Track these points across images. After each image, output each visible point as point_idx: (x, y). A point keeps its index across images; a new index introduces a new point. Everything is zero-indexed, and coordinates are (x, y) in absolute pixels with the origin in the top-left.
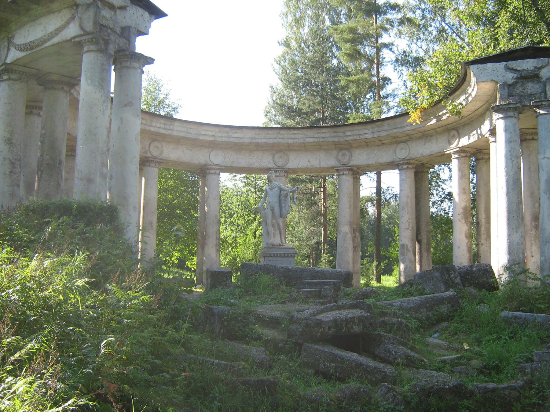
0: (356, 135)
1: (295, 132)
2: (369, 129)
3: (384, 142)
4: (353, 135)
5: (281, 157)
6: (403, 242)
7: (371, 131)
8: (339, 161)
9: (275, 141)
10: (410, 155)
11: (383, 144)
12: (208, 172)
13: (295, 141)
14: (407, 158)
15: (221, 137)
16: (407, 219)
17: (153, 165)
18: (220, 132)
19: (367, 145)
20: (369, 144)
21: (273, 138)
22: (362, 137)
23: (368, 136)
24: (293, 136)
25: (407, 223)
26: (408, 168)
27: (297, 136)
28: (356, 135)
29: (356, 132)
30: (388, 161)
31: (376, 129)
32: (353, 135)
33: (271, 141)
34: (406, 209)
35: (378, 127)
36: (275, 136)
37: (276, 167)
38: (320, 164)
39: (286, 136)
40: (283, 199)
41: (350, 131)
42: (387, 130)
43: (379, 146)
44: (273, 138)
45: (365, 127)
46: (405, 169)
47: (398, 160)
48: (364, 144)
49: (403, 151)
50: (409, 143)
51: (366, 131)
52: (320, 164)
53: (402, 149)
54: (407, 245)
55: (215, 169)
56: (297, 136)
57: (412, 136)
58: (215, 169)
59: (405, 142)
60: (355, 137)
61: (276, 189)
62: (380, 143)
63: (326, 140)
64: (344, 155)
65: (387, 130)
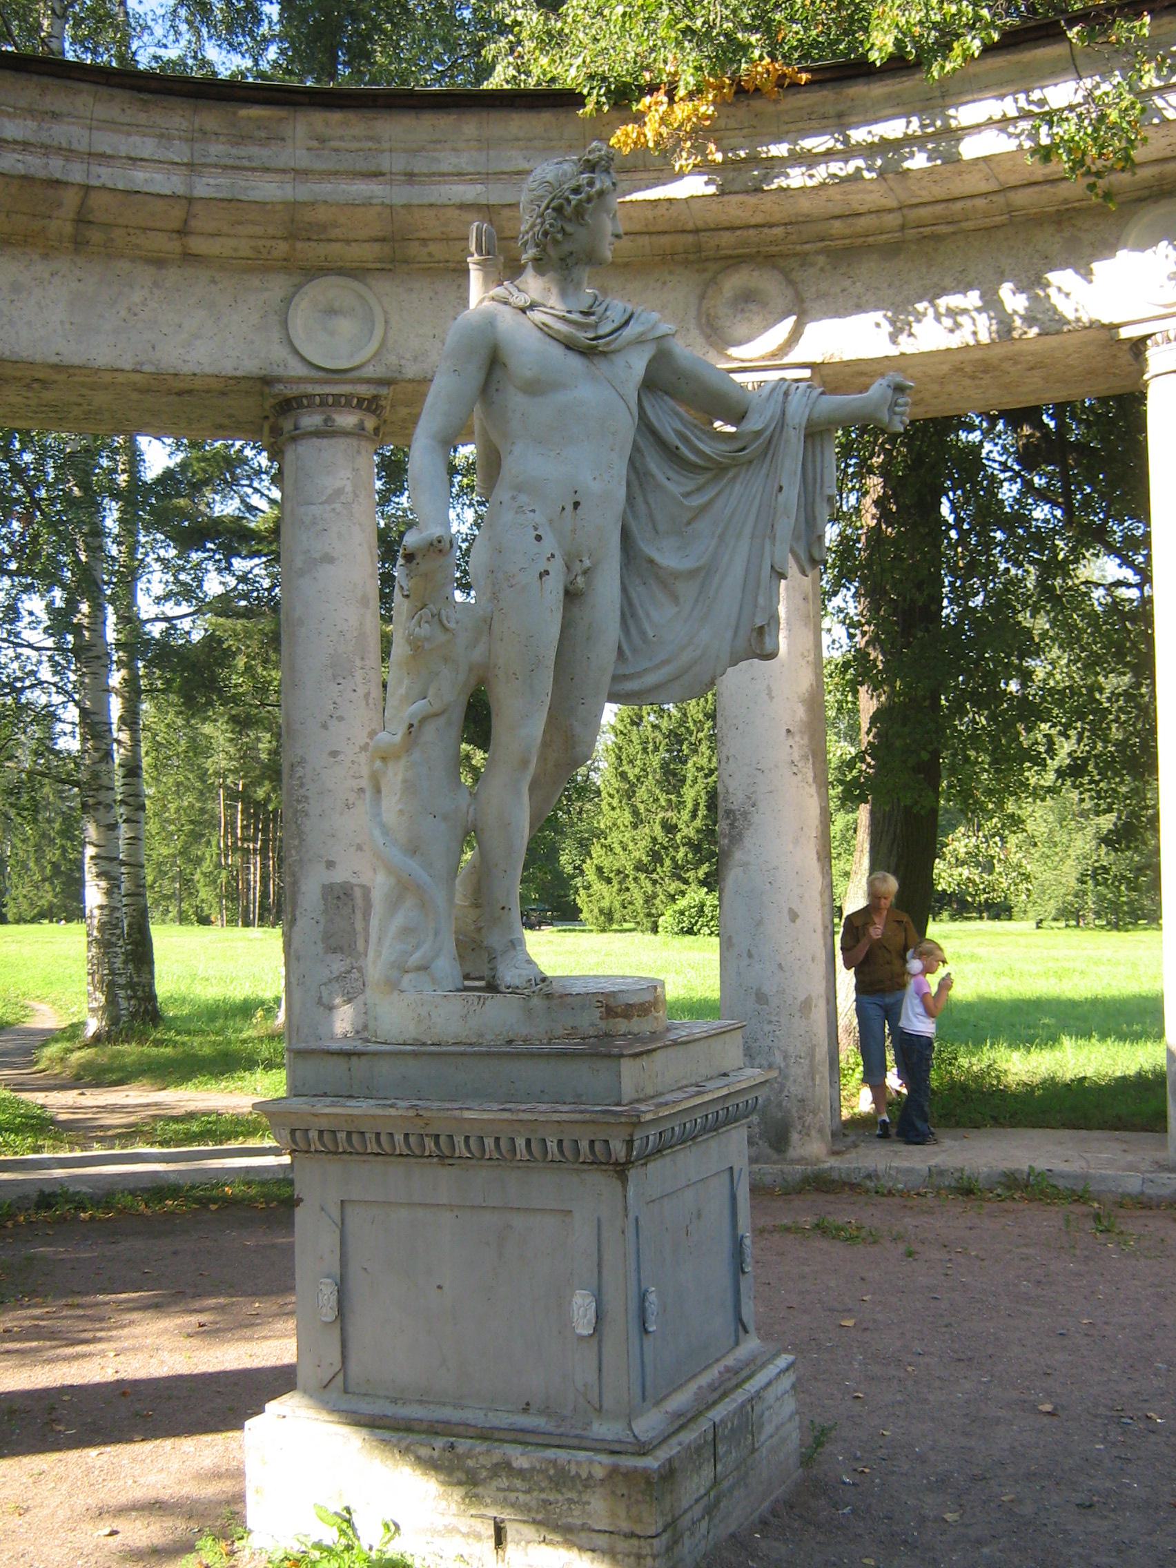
0: (69, 153)
2: (164, 137)
3: (197, 245)
4: (47, 149)
6: (340, 875)
7: (179, 152)
10: (392, 359)
11: (189, 258)
14: (369, 372)
16: (362, 738)
19: (79, 244)
20: (96, 236)
22: (104, 175)
23: (141, 178)
25: (363, 758)
26: (358, 432)
28: (69, 153)
29: (61, 133)
30: (228, 367)
31: (217, 150)
32: (47, 149)
34: (359, 674)
35: (241, 139)
41: (31, 112)
42: (301, 174)
43: (159, 262)
45: (142, 118)
46: (345, 433)
47: (299, 370)
48: (62, 224)
49: (346, 327)
50: (383, 285)
51: (147, 147)
53: (331, 312)
54: (366, 891)
57: (414, 249)
59: (356, 272)
60: (56, 167)
62: (174, 246)
65: (301, 174)
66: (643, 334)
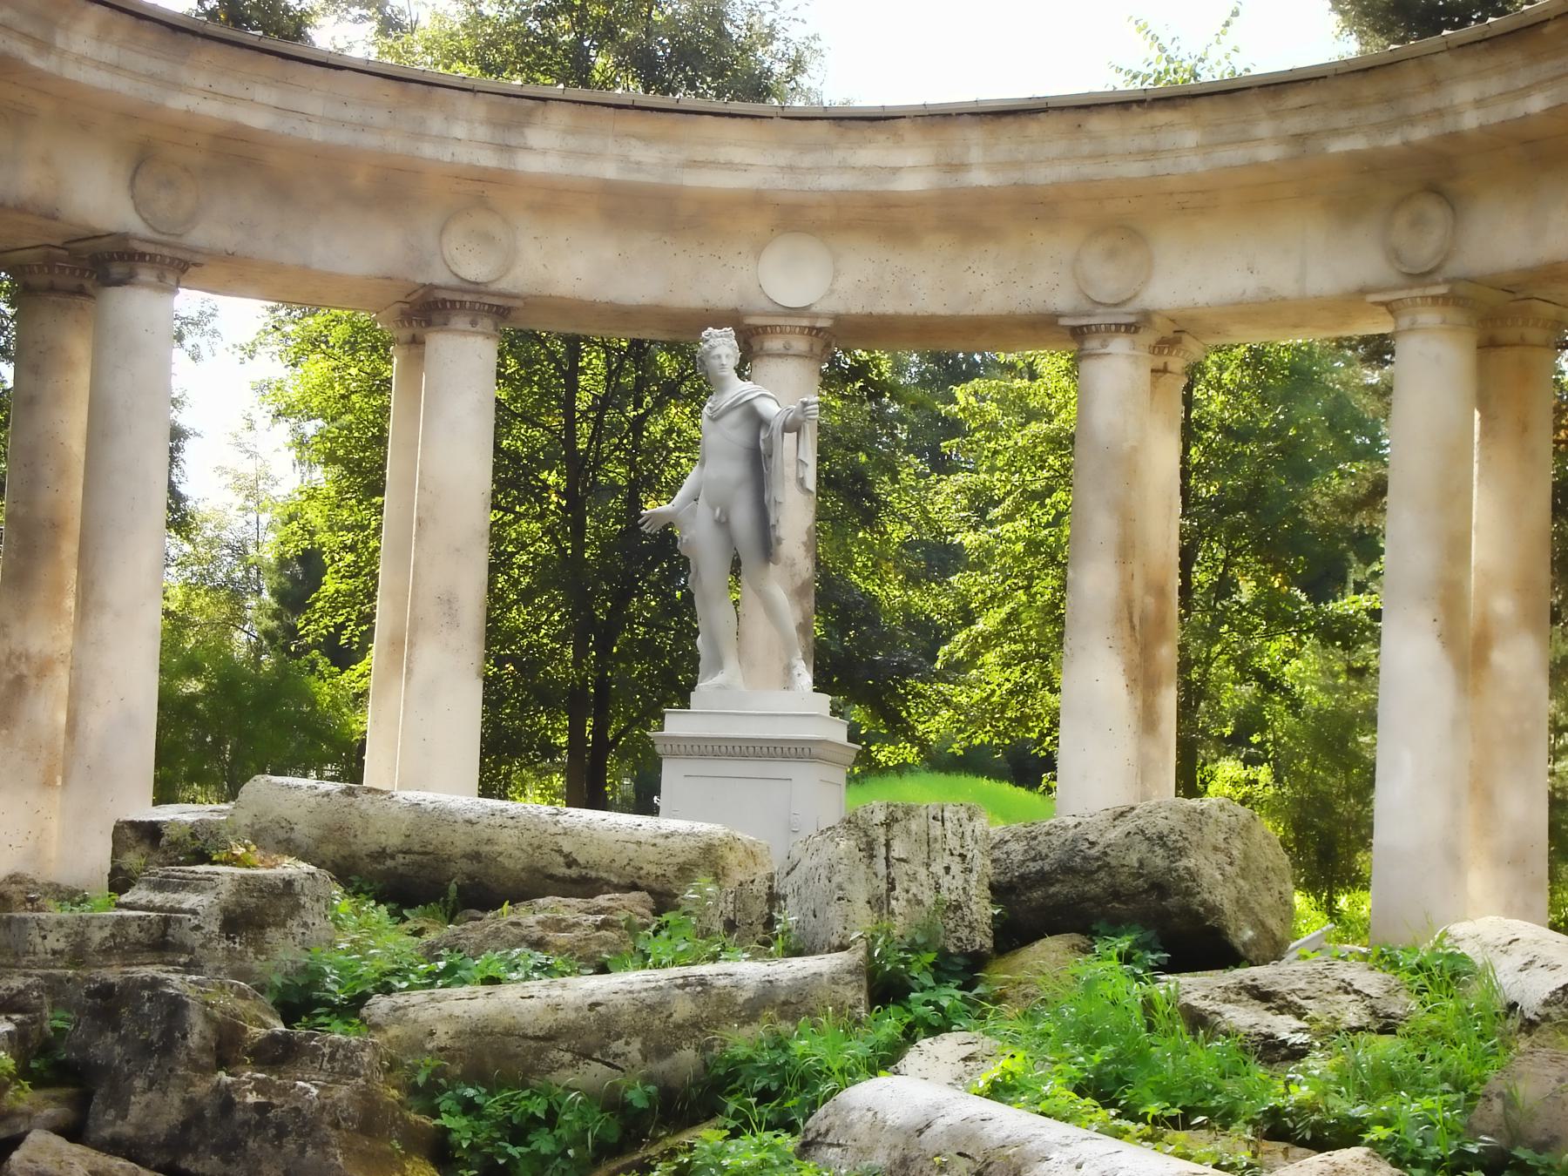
8: (1394, 255)
15: (791, 168)
17: (460, 322)
37: (1087, 306)
55: (782, 330)
58: (782, 330)
61: (734, 417)
64: (1418, 223)
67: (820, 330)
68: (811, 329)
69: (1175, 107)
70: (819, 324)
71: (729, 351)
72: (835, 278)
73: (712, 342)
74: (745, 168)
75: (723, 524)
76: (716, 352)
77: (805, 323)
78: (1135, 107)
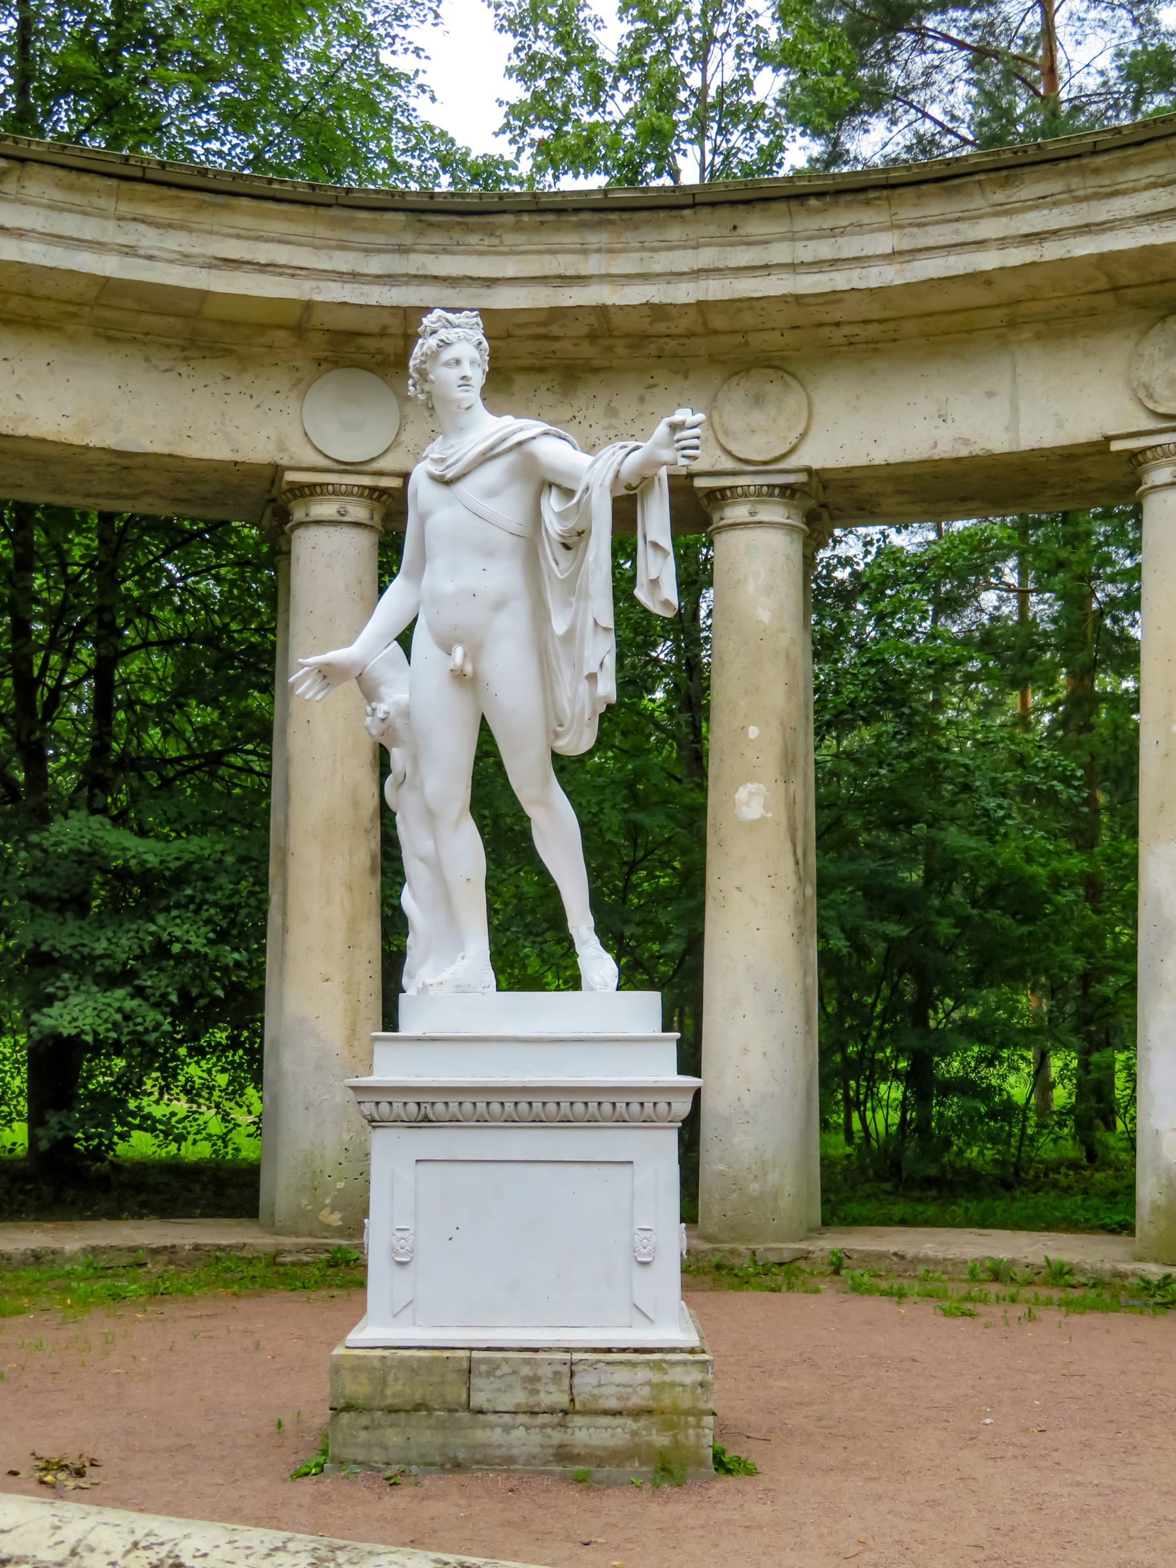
1: (843, 217)
5: (758, 400)
8: (1142, 395)
9: (715, 290)
12: (298, 515)
13: (841, 280)
15: (354, 277)
18: (343, 247)
21: (697, 274)
24: (825, 249)
27: (849, 247)
33: (684, 293)
36: (707, 257)
37: (728, 464)
38: (1012, 426)
39: (780, 253)
40: (556, 565)
44: (697, 274)
52: (1012, 426)
56: (849, 247)
61: (492, 473)
63: (1052, 251)
66: (492, 448)
67: (384, 491)
68: (373, 489)
69: (868, 203)
70: (385, 482)
71: (476, 354)
72: (401, 428)
73: (443, 334)
74: (295, 272)
75: (465, 680)
76: (448, 355)
77: (366, 481)
78: (813, 202)
